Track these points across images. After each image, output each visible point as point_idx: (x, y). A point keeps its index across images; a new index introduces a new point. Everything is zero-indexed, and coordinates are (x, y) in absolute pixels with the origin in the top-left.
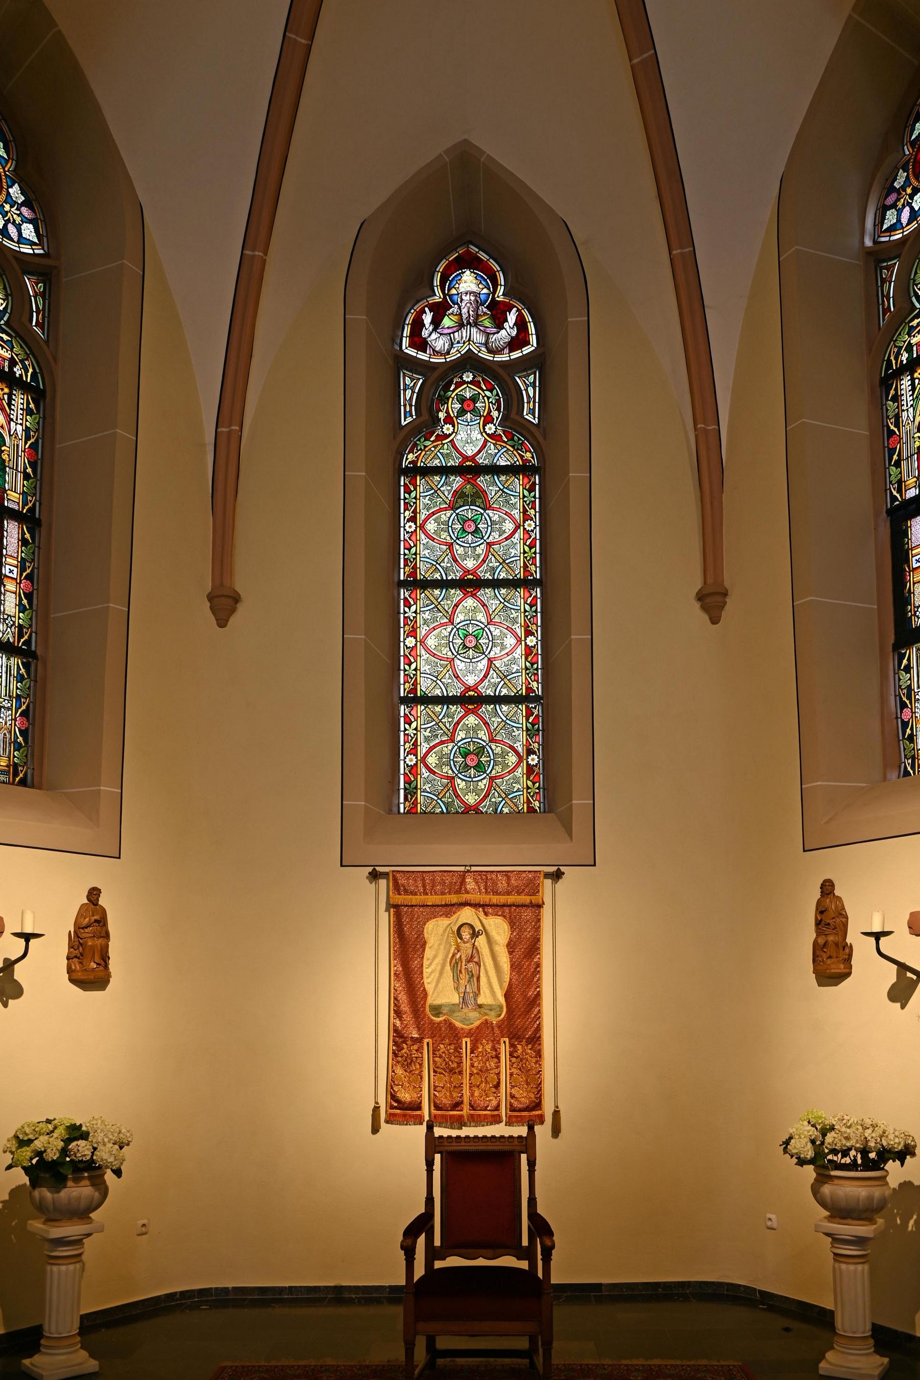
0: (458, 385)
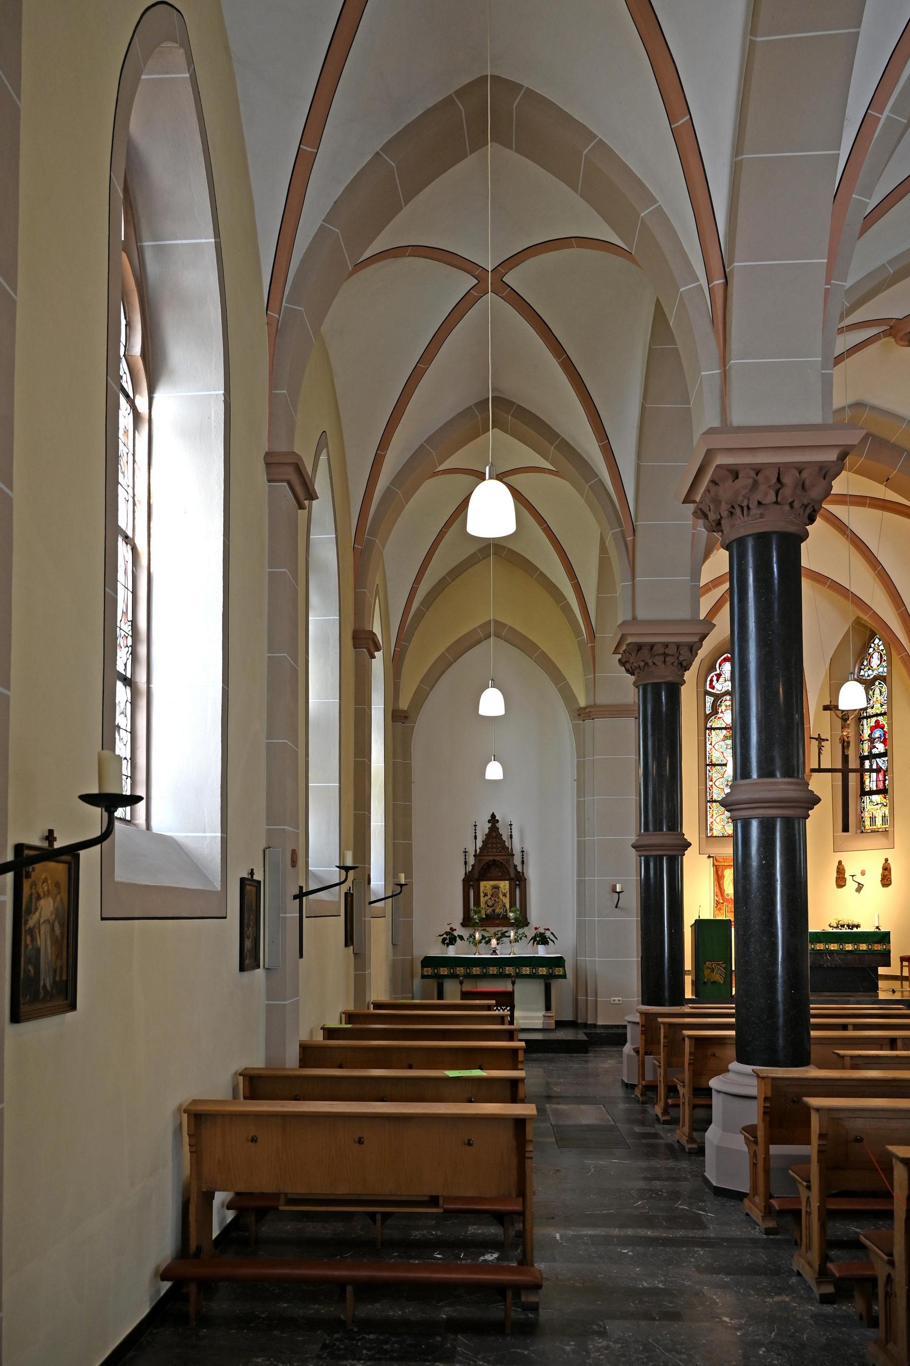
0: (725, 701)
